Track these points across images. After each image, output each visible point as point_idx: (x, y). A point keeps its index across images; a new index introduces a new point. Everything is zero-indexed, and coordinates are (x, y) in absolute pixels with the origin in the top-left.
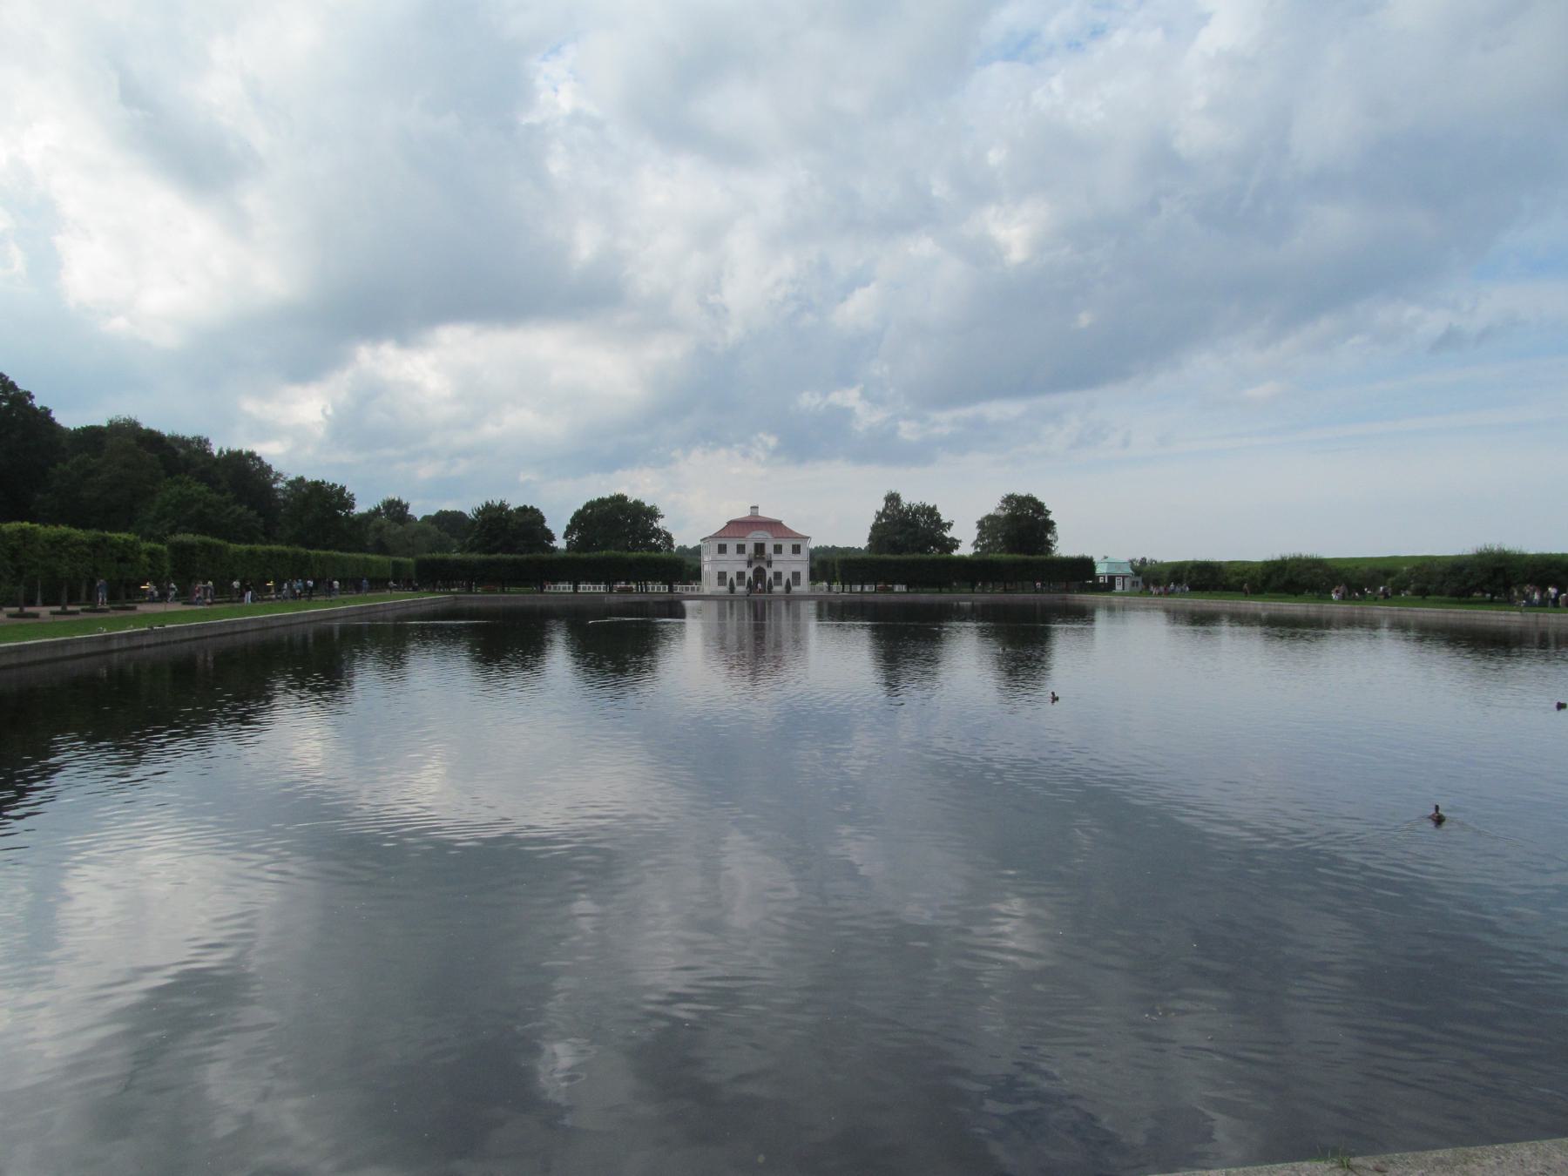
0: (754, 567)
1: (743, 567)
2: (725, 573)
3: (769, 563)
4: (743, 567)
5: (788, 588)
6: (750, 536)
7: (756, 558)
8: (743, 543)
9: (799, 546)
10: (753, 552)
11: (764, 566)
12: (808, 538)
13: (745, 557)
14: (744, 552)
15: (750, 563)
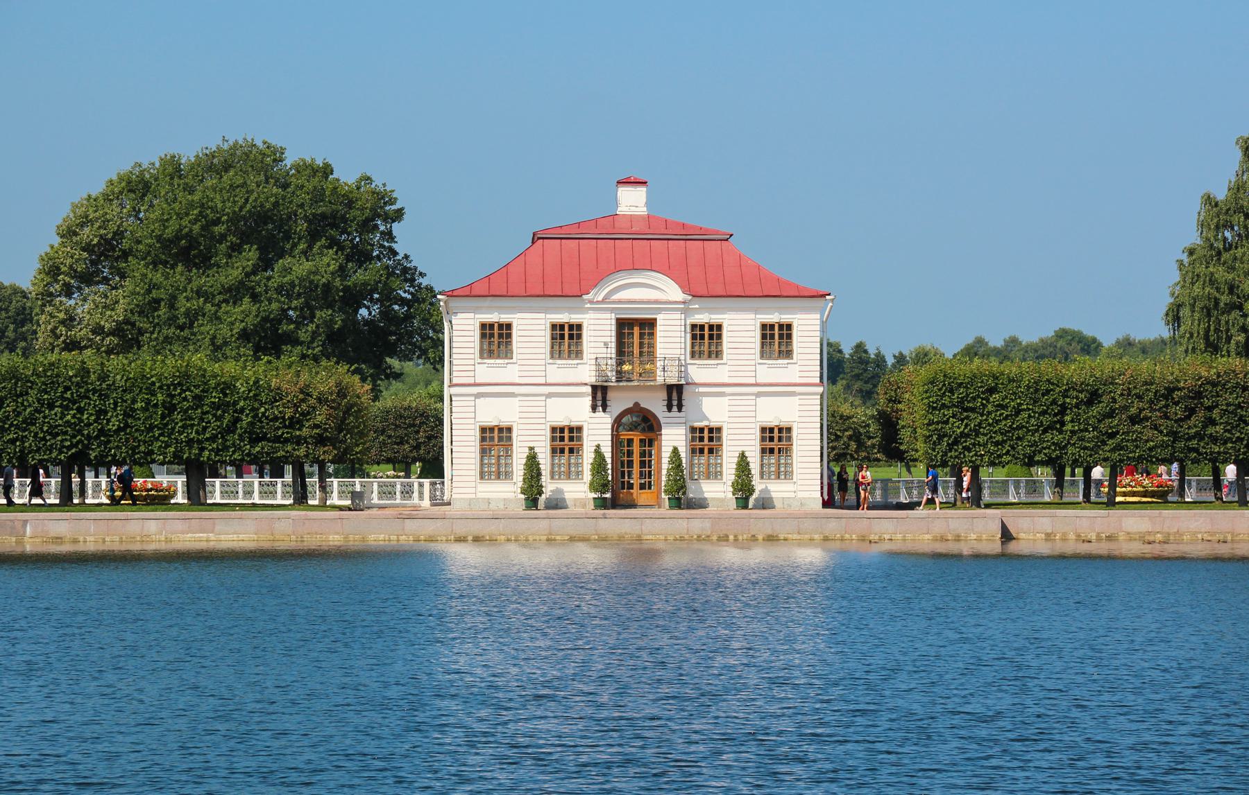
0: (620, 402)
1: (577, 410)
2: (509, 430)
3: (675, 394)
4: (577, 410)
5: (743, 489)
6: (599, 294)
7: (620, 375)
8: (574, 318)
9: (786, 330)
10: (612, 350)
11: (656, 405)
12: (823, 296)
13: (585, 372)
14: (579, 354)
15: (600, 396)
